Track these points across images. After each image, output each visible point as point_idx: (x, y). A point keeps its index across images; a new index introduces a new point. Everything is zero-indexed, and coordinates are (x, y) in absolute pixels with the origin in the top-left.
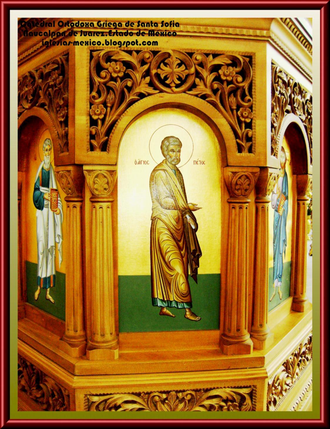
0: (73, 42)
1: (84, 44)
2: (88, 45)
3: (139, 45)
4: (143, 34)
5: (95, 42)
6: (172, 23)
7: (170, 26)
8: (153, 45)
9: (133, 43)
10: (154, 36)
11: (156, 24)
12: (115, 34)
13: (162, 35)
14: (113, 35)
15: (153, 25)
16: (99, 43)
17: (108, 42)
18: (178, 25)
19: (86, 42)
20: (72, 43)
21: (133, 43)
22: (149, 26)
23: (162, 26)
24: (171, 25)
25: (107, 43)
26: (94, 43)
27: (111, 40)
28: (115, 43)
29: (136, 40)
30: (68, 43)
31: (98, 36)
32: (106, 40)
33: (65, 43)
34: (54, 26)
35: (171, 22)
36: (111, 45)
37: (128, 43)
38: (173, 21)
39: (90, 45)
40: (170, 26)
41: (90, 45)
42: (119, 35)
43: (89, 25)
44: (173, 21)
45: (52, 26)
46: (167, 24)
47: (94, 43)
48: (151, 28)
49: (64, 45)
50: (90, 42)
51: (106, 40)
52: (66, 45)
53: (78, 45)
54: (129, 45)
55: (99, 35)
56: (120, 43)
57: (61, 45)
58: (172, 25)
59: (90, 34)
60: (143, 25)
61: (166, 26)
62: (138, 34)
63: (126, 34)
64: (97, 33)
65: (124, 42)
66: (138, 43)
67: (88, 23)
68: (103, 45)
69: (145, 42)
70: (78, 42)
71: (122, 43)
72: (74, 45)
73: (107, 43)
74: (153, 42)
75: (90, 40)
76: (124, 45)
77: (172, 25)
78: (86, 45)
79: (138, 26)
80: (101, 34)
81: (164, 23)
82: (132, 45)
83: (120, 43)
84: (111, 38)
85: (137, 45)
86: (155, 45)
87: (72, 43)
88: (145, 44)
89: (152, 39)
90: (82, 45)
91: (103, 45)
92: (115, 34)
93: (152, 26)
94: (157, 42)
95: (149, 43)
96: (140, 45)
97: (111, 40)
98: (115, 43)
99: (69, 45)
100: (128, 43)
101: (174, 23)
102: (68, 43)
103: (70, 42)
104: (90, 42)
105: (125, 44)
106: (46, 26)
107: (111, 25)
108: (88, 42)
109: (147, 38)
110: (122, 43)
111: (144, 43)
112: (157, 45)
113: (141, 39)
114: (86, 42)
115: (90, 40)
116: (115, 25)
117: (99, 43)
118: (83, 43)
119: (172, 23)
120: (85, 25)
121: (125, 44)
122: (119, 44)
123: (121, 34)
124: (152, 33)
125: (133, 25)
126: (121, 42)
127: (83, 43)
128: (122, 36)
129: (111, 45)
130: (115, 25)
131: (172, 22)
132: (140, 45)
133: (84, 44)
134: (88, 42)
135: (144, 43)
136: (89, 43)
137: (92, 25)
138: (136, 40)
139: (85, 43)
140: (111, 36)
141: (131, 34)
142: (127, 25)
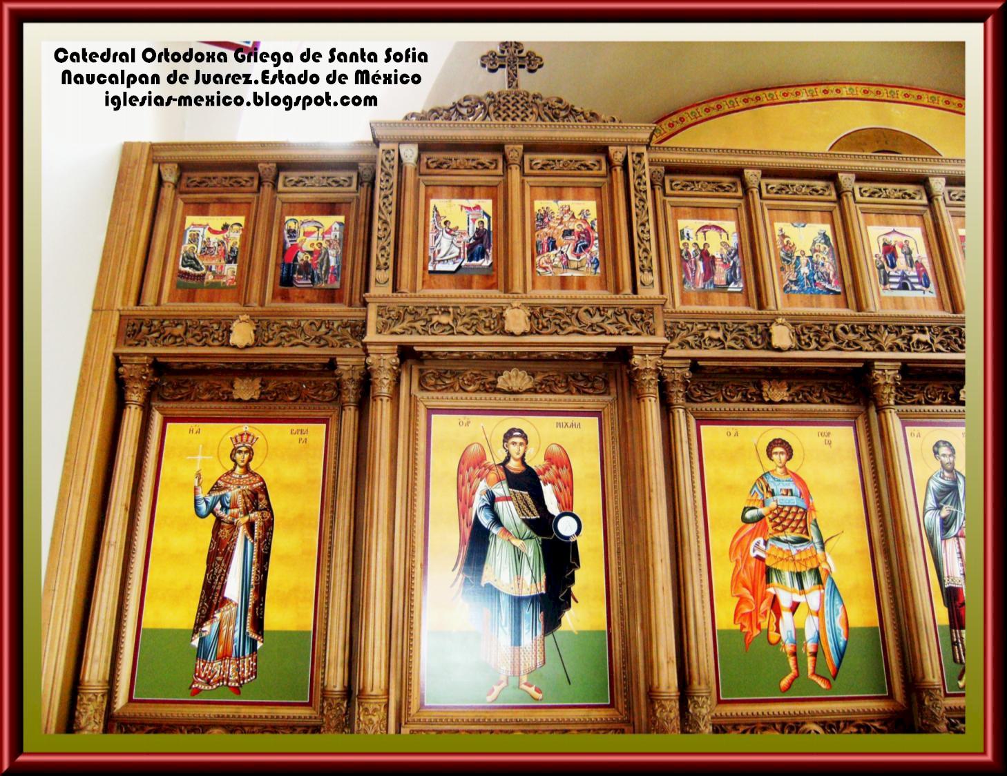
0: (177, 97)
1: (203, 103)
2: (213, 104)
3: (332, 104)
4: (343, 78)
5: (229, 98)
6: (410, 53)
7: (407, 61)
8: (365, 104)
9: (319, 101)
10: (368, 82)
11: (373, 57)
12: (277, 80)
13: (387, 79)
14: (273, 82)
15: (366, 57)
16: (239, 101)
17: (260, 98)
18: (423, 57)
19: (207, 97)
20: (175, 100)
21: (319, 101)
22: (357, 61)
23: (387, 60)
24: (408, 56)
25: (258, 101)
26: (227, 101)
27: (267, 94)
28: (276, 101)
29: (327, 94)
30: (165, 101)
31: (238, 83)
32: (255, 94)
33: (159, 101)
34: (133, 60)
35: (408, 50)
36: (267, 104)
37: (307, 101)
38: (414, 49)
39: (219, 104)
40: (407, 61)
41: (219, 104)
42: (285, 82)
43: (216, 57)
44: (414, 49)
45: (127, 61)
46: (398, 57)
47: (227, 101)
48: (361, 66)
49: (157, 104)
50: (219, 98)
51: (255, 94)
52: (162, 104)
53: (190, 104)
54: (309, 104)
55: (239, 81)
56: (287, 101)
57: (150, 104)
58: (410, 60)
59: (218, 79)
60: (342, 57)
61: (399, 61)
62: (331, 78)
63: (304, 78)
64: (235, 78)
65: (299, 98)
66: (332, 101)
67: (213, 53)
68: (248, 104)
69: (347, 98)
70: (189, 98)
71: (294, 100)
72: (180, 104)
73: (258, 101)
74: (367, 98)
75: (218, 93)
76: (296, 104)
77: (410, 60)
78: (207, 104)
79: (331, 60)
80: (243, 79)
81: (392, 54)
82: (317, 104)
83: (287, 101)
84: (268, 88)
85: (329, 104)
86: (370, 104)
87: (175, 100)
88: (348, 103)
89: (364, 90)
90: (200, 105)
91: (248, 104)
92: (277, 80)
93: (364, 60)
94: (375, 98)
95: (357, 101)
96: (336, 104)
97: (267, 94)
98: (276, 101)
99: (168, 104)
100: (307, 101)
101: (414, 54)
102: (165, 101)
103: (170, 99)
104: (219, 98)
105: (301, 102)
106: (114, 60)
107: (267, 59)
108: (213, 97)
109: (352, 89)
110: (294, 100)
111: (345, 101)
112: (376, 104)
113: (337, 91)
114: (207, 97)
115: (218, 93)
116: (276, 57)
117: (239, 101)
118: (202, 100)
119: (410, 55)
120: (206, 57)
121: (301, 102)
122: (285, 103)
123: (291, 79)
124: (362, 77)
125: (319, 59)
126: (289, 98)
127: (202, 100)
128: (294, 83)
129: (267, 104)
130: (276, 57)
131: (411, 51)
132: (336, 104)
133: (203, 103)
134: (213, 97)
135: (345, 101)
136: (215, 100)
137: (222, 57)
138: (327, 94)
139: (205, 100)
140: (266, 83)
141: (315, 79)
142: (305, 57)
